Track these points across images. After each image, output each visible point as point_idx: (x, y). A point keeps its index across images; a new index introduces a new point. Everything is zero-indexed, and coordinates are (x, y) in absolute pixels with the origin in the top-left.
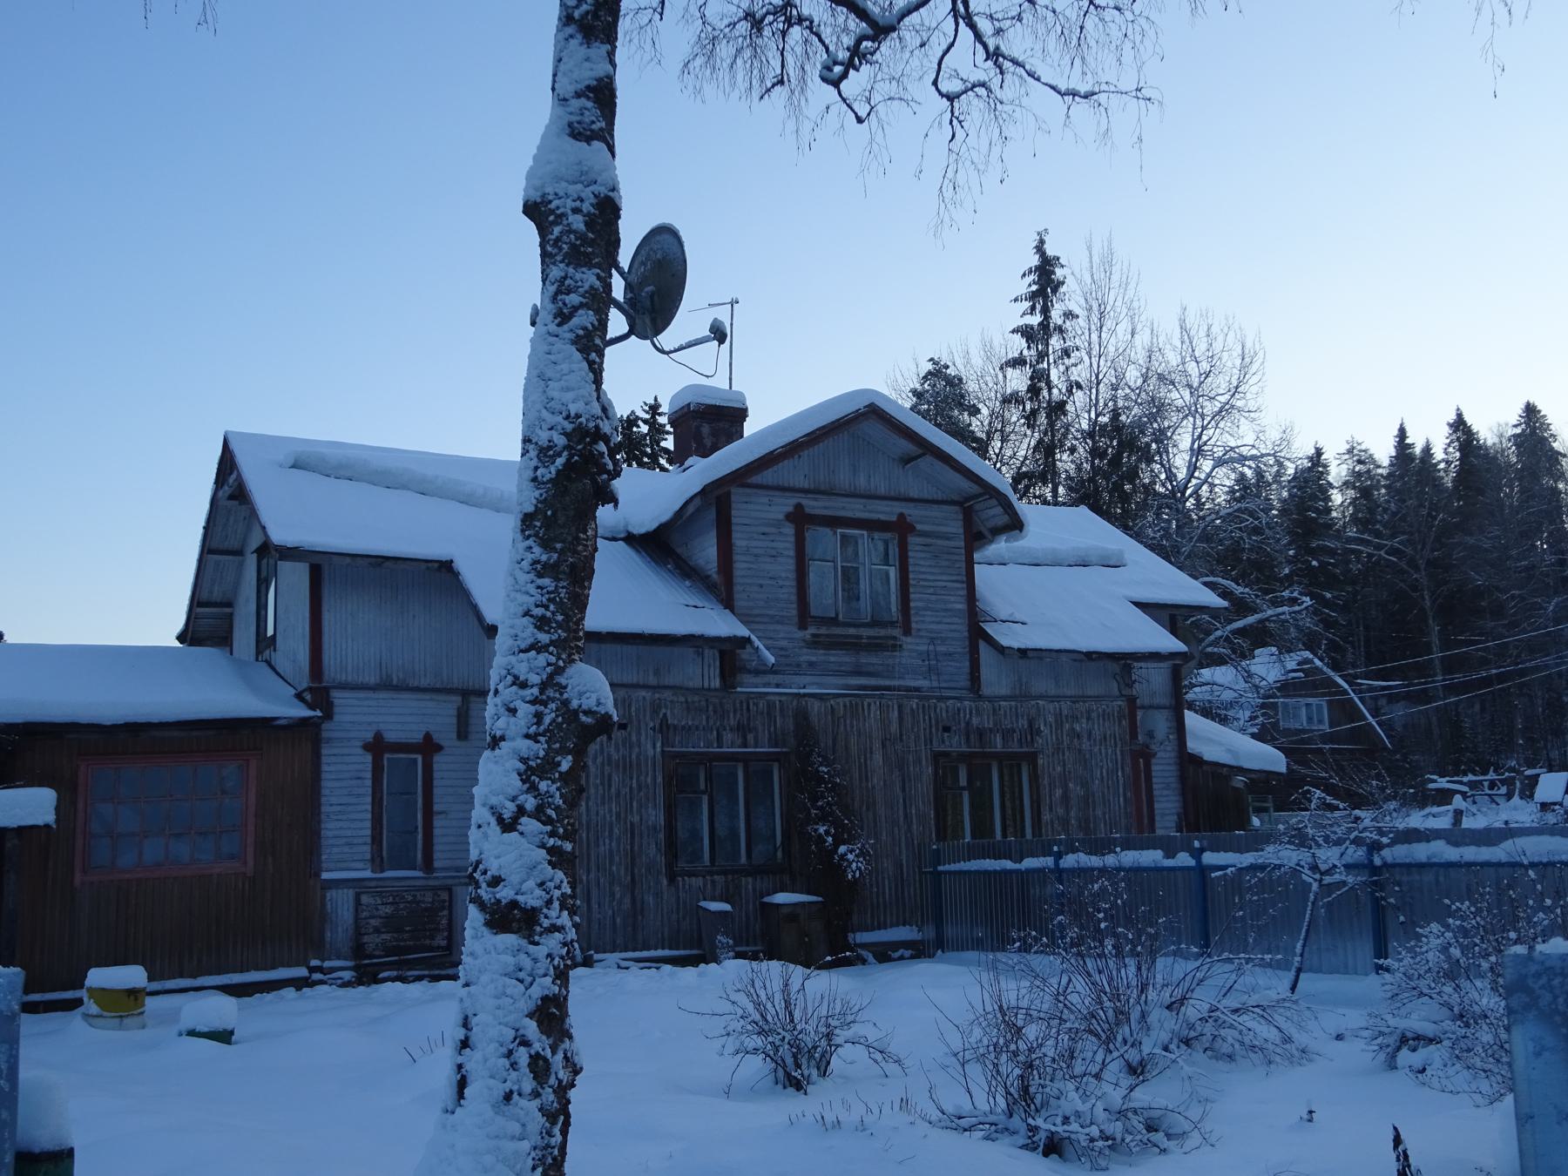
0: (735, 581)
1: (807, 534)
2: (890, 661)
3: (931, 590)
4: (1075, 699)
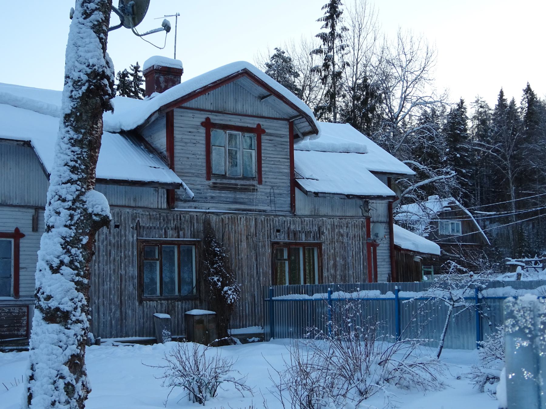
0: (175, 155)
1: (211, 133)
2: (251, 197)
3: (272, 163)
4: (341, 218)
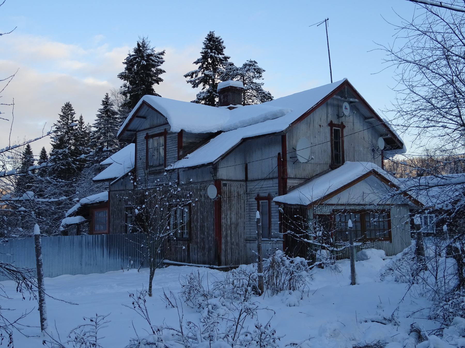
4: (202, 183)
